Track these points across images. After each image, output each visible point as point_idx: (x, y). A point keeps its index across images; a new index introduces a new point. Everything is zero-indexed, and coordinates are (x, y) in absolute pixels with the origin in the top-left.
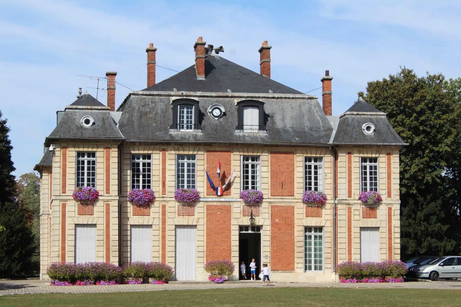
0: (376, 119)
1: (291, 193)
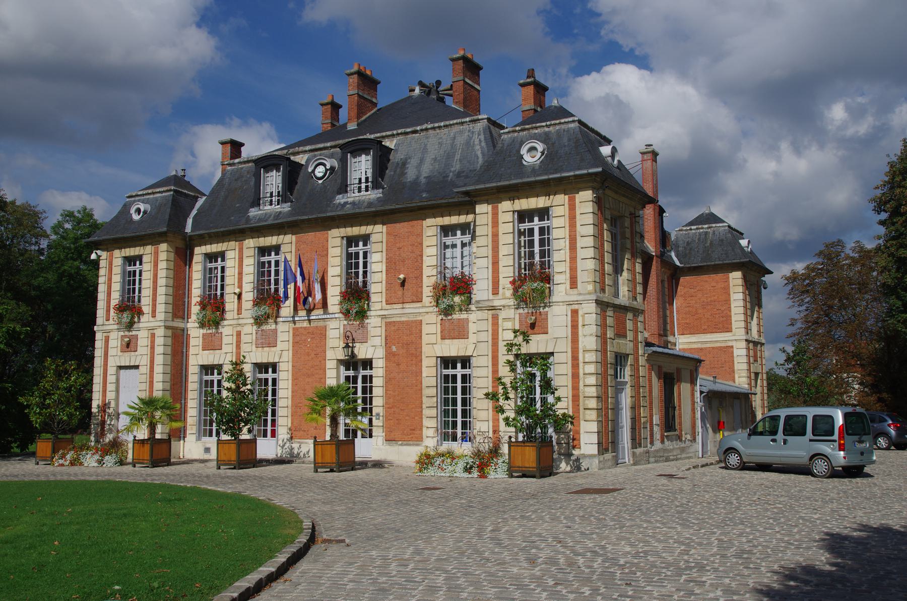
0: (558, 132)
1: (417, 296)
